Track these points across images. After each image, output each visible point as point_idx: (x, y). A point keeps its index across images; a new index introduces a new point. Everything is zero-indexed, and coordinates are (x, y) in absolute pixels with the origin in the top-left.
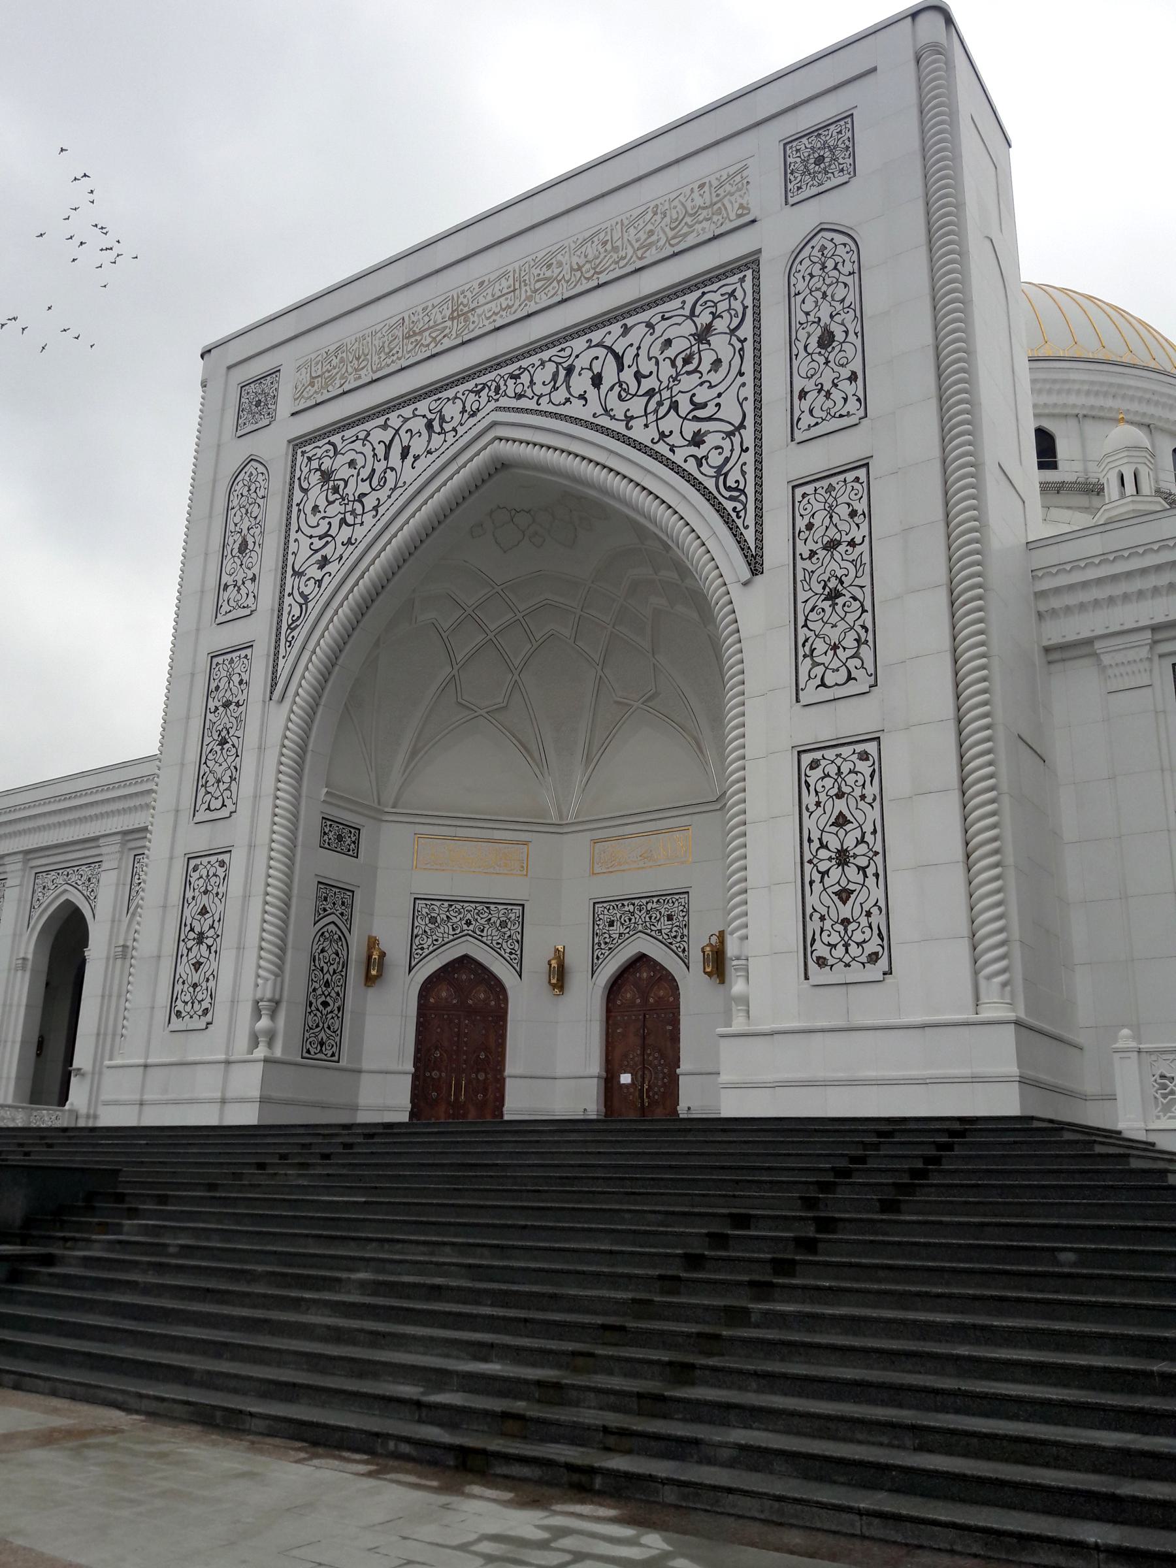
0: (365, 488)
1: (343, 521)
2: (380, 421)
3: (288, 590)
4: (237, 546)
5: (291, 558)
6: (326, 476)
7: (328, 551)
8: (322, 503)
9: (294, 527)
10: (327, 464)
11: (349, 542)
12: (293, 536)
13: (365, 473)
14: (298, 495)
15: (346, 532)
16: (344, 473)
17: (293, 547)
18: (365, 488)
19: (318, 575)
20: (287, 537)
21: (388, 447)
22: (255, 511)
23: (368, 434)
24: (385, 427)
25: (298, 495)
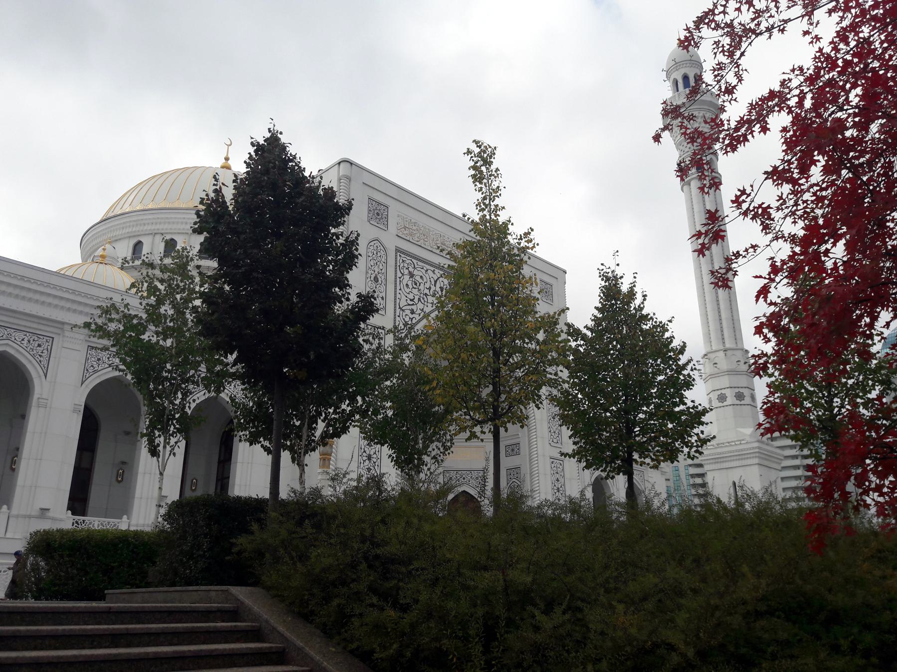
0: (427, 291)
1: (419, 300)
2: (433, 269)
3: (397, 314)
4: (373, 276)
5: (398, 301)
6: (411, 275)
7: (414, 307)
8: (411, 286)
9: (398, 288)
10: (411, 269)
11: (422, 310)
12: (398, 291)
13: (427, 285)
14: (399, 275)
15: (420, 306)
16: (418, 278)
17: (398, 296)
18: (427, 291)
19: (411, 316)
20: (395, 292)
21: (436, 282)
22: (381, 267)
23: (427, 271)
24: (433, 271)
25: (399, 275)
